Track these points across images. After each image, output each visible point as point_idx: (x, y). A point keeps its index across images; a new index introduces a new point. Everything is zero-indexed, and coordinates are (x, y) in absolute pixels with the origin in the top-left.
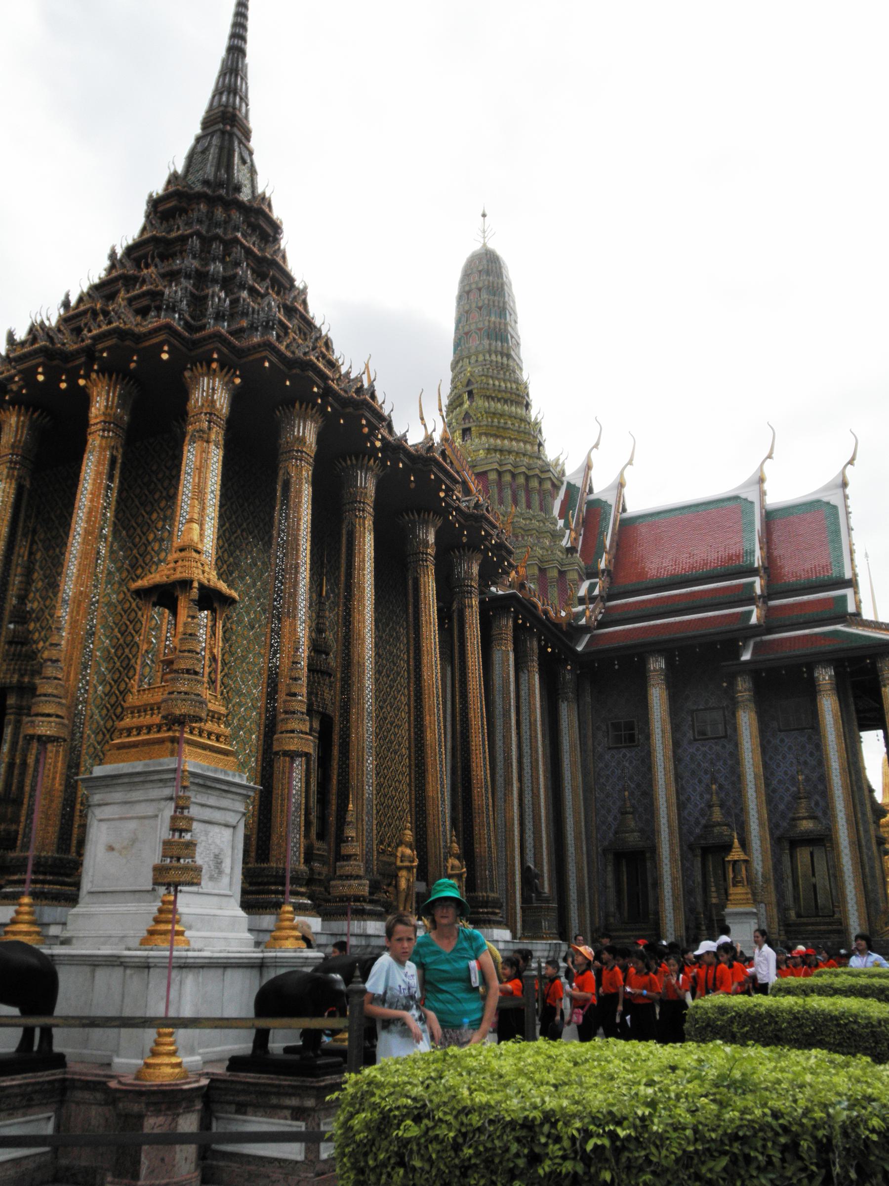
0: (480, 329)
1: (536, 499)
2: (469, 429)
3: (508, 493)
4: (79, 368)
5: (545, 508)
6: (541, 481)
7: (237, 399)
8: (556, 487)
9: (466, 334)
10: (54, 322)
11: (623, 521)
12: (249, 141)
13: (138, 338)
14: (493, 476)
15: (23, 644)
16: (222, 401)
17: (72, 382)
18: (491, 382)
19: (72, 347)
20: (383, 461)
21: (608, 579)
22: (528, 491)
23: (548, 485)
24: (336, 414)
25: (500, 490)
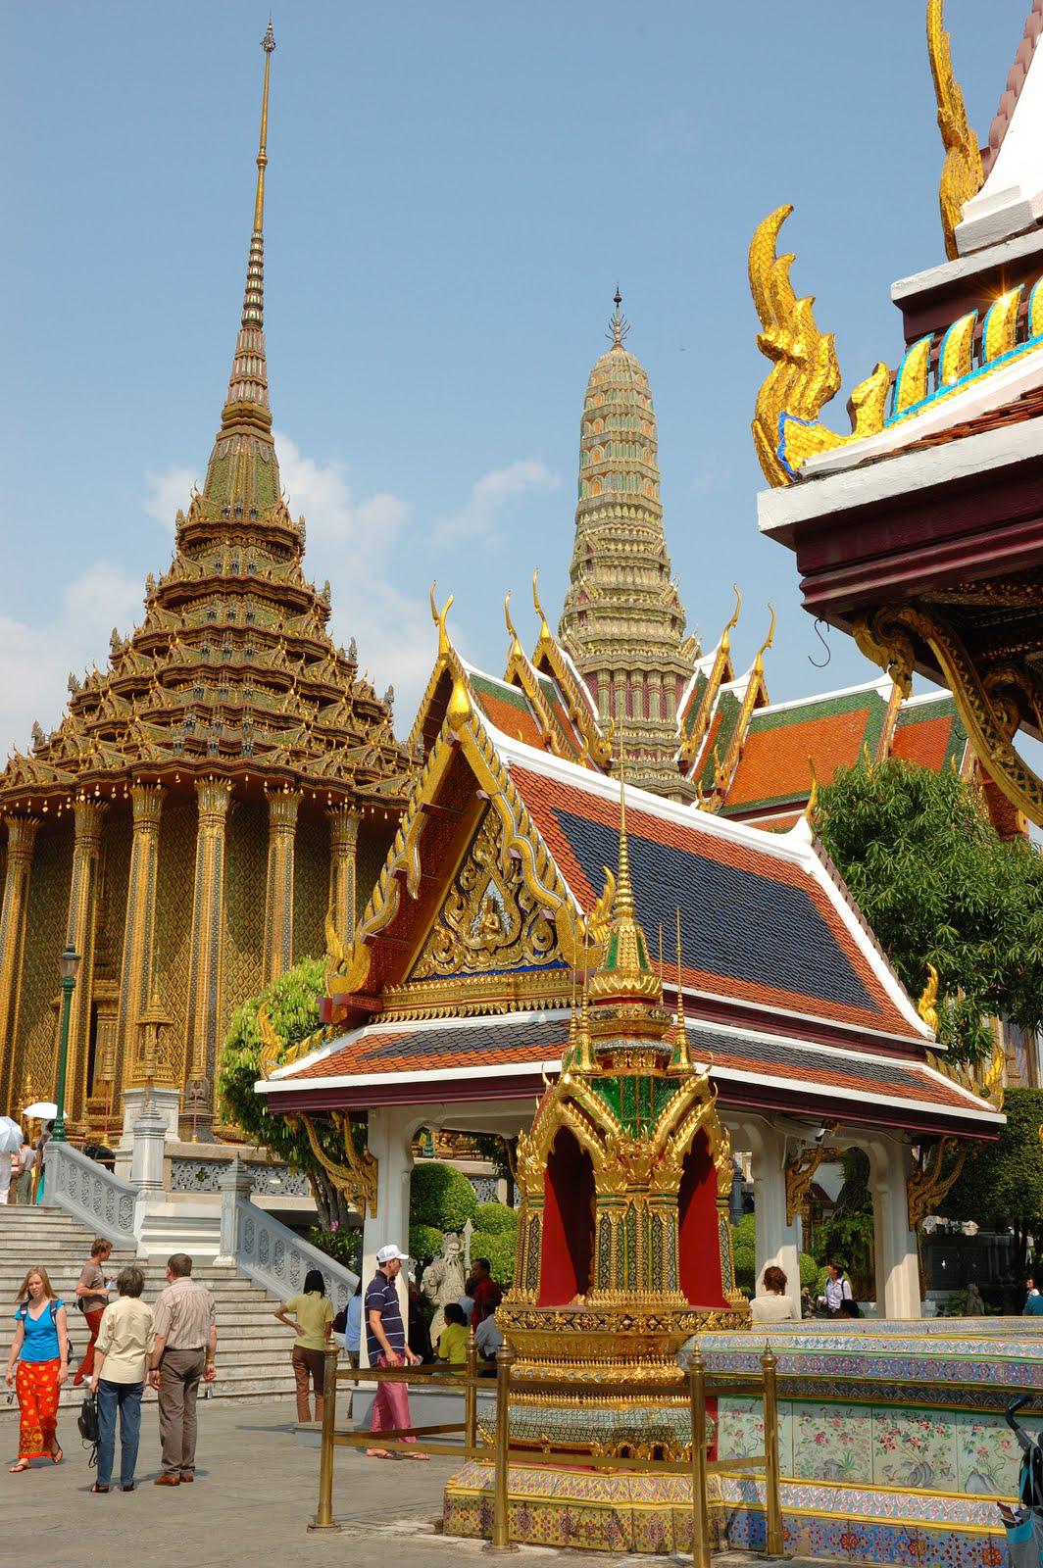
0: (604, 474)
1: (656, 697)
2: (585, 612)
3: (621, 695)
4: (122, 784)
5: (664, 713)
6: (663, 676)
7: (233, 796)
8: (682, 679)
9: (589, 479)
10: (104, 667)
11: (754, 722)
12: (267, 431)
13: (158, 767)
14: (603, 678)
15: (105, 965)
16: (222, 805)
17: (120, 792)
18: (613, 547)
19: (116, 768)
20: (359, 808)
21: (718, 798)
22: (647, 691)
23: (671, 681)
24: (308, 793)
25: (612, 693)
